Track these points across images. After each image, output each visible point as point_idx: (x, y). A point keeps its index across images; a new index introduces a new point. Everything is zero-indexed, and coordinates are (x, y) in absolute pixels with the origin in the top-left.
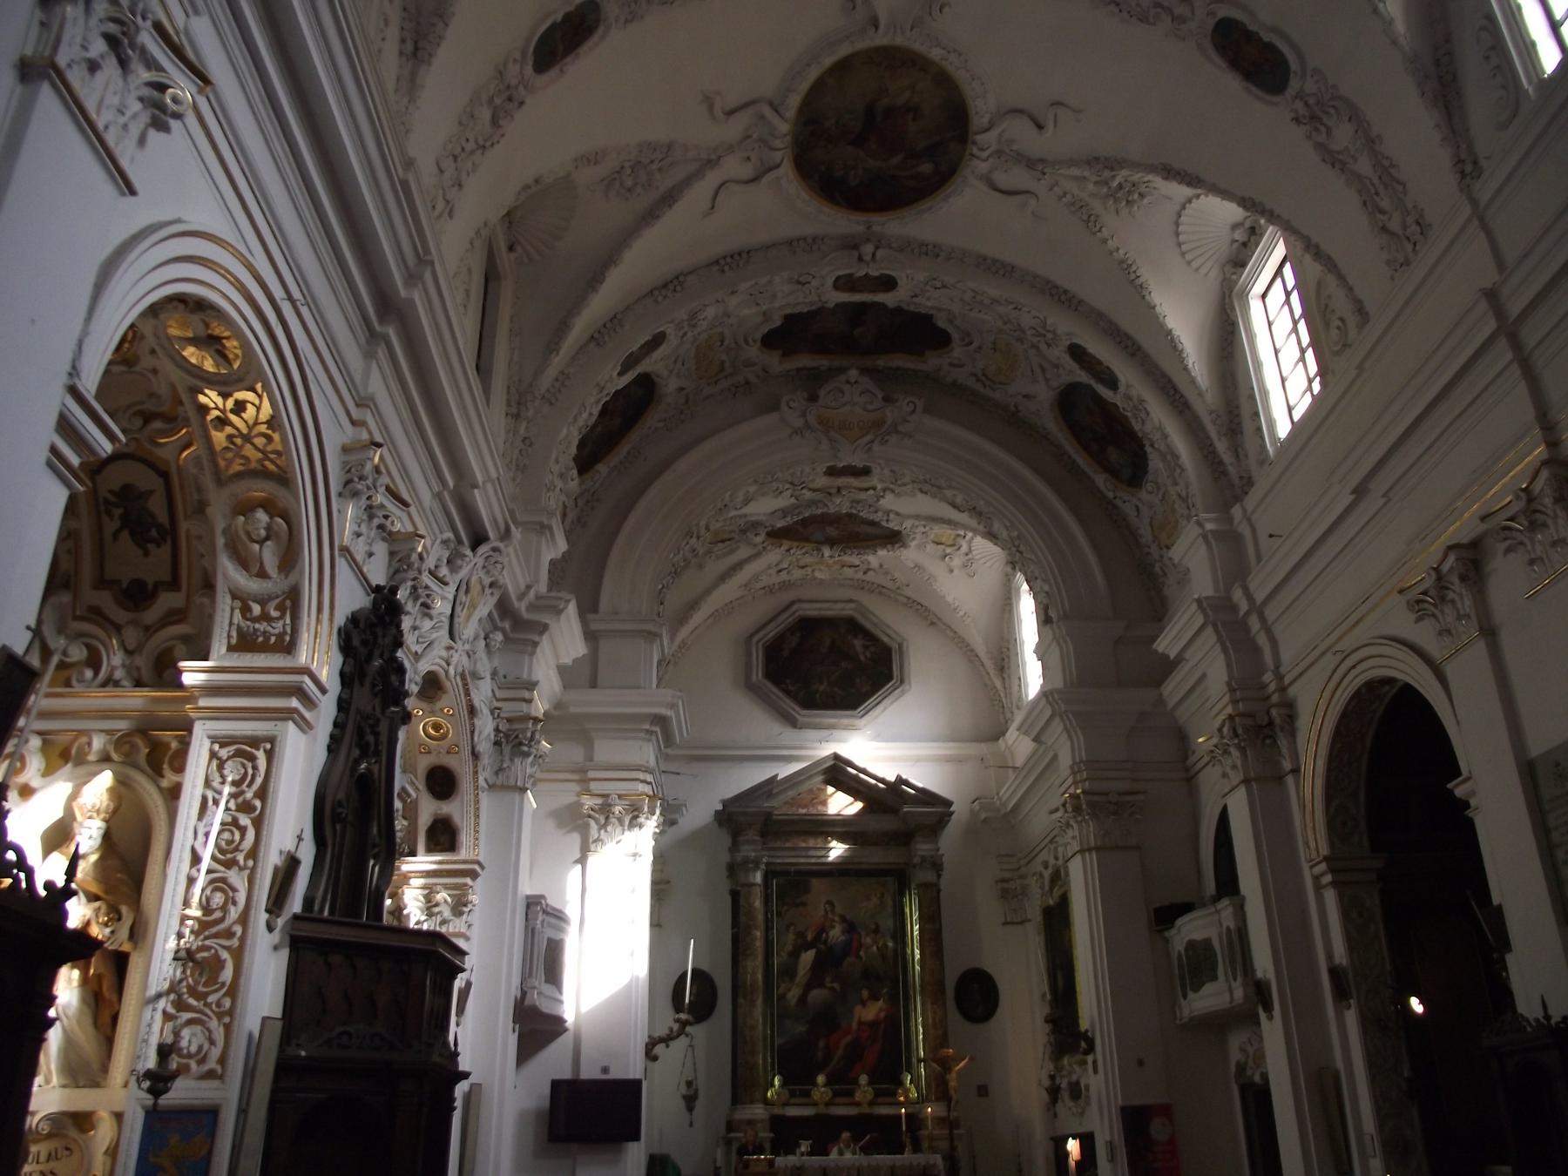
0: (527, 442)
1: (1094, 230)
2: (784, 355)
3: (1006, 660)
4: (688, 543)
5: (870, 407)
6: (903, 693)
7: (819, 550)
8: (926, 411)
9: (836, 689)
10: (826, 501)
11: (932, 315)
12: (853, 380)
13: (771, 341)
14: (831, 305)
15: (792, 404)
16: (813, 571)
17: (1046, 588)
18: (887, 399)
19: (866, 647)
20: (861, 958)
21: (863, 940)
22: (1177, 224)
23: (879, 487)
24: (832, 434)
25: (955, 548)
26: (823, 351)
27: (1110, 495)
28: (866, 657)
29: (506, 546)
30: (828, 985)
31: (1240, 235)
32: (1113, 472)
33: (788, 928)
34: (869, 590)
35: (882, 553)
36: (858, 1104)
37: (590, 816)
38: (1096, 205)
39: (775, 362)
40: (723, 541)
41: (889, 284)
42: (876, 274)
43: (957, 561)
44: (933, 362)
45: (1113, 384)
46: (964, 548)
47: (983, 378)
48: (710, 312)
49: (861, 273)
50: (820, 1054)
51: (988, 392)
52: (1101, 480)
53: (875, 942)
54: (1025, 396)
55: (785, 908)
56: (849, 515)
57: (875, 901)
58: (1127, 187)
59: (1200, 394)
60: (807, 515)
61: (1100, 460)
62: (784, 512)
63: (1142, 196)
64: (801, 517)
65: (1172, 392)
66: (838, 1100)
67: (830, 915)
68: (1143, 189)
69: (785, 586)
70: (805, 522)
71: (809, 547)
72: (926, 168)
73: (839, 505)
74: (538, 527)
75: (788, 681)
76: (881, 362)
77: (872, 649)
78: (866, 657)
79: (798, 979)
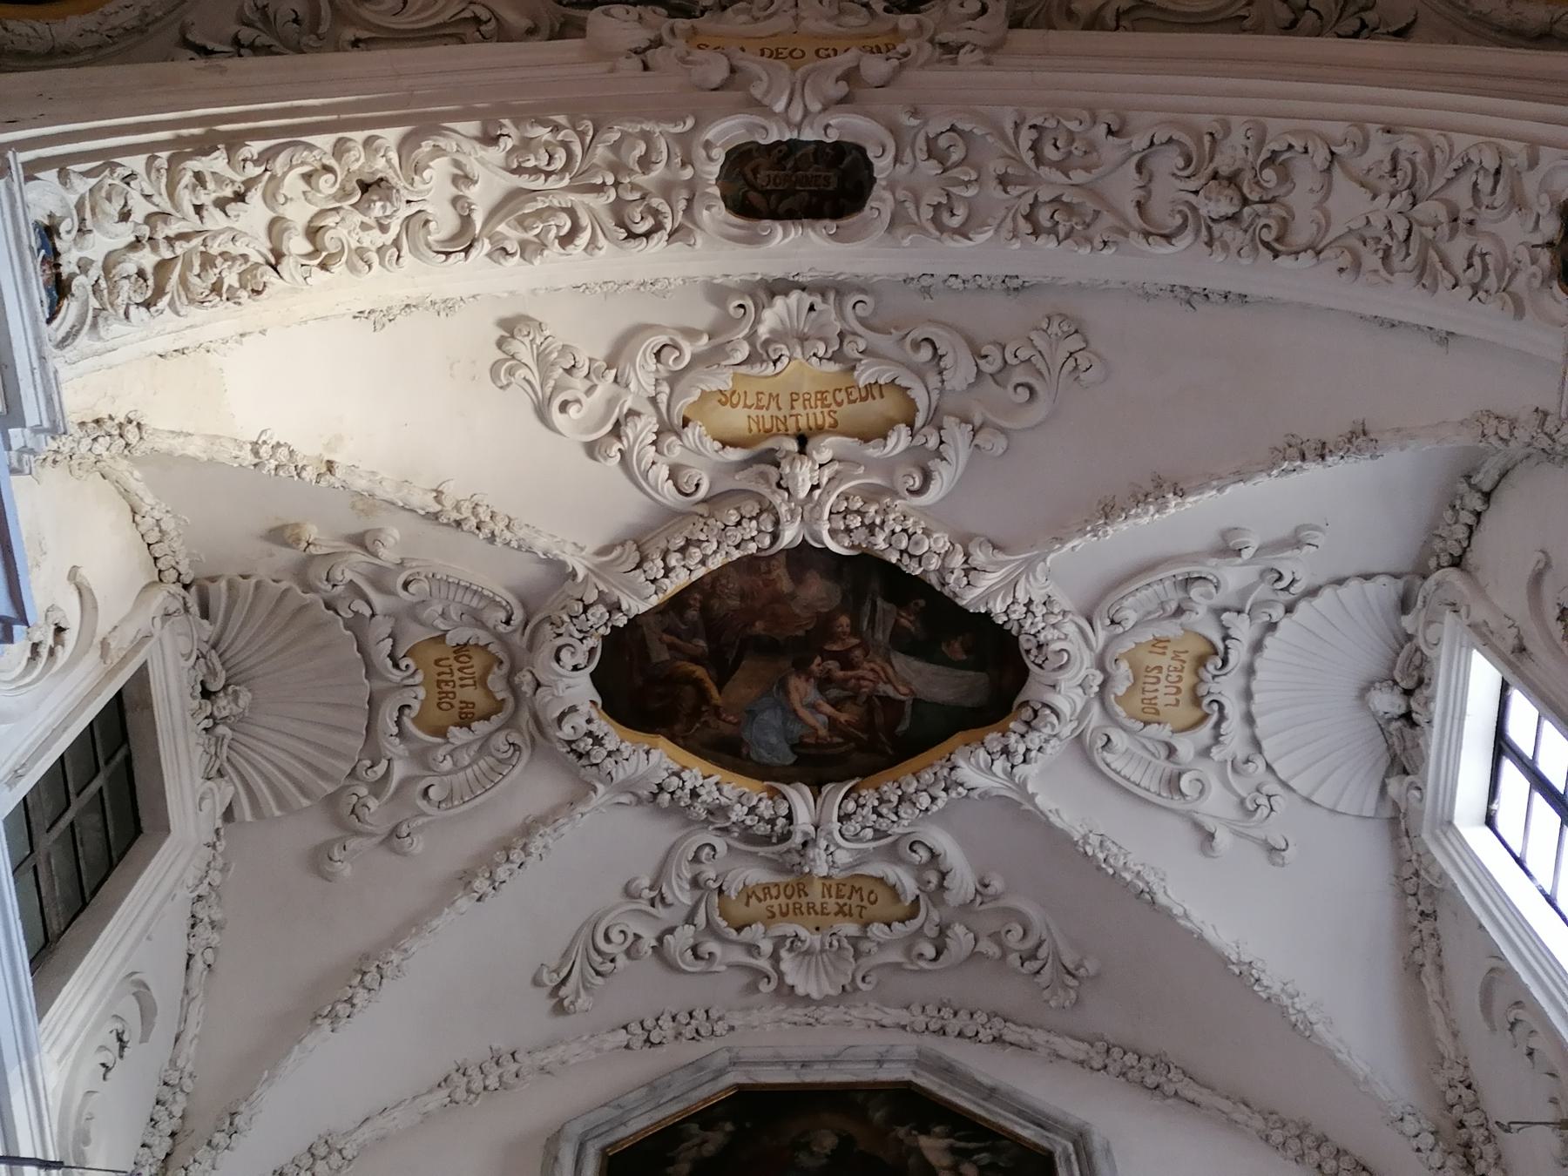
7: (774, 794)
10: (764, 490)
19: (961, 1155)
34: (960, 1034)
40: (465, 722)
69: (691, 1024)
77: (984, 1158)
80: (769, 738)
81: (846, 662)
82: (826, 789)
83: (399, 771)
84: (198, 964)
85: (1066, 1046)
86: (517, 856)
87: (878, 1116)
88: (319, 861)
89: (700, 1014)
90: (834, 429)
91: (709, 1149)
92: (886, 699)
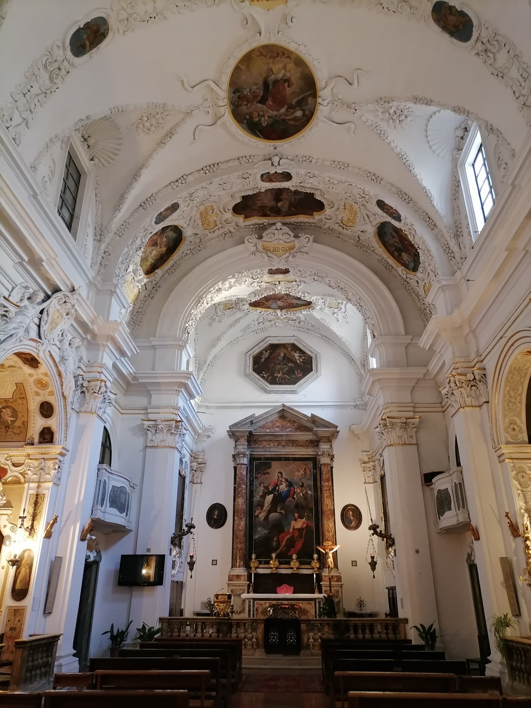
0: (107, 254)
1: (383, 138)
2: (246, 217)
3: (366, 361)
4: (201, 306)
5: (288, 241)
6: (317, 377)
8: (315, 241)
9: (285, 376)
11: (313, 194)
12: (279, 228)
13: (238, 209)
14: (263, 190)
15: (250, 240)
16: (275, 323)
17: (373, 322)
18: (296, 236)
20: (294, 498)
21: (296, 490)
22: (426, 131)
23: (298, 280)
24: (269, 254)
25: (339, 309)
26: (265, 215)
27: (405, 277)
28: (300, 361)
29: (72, 295)
30: (279, 511)
31: (460, 133)
32: (406, 266)
33: (260, 485)
35: (304, 312)
36: (292, 568)
37: (148, 430)
38: (383, 125)
39: (240, 219)
41: (287, 177)
42: (281, 172)
43: (340, 316)
44: (317, 217)
45: (398, 218)
46: (343, 310)
47: (342, 224)
48: (201, 193)
49: (272, 172)
50: (275, 544)
51: (345, 231)
52: (400, 269)
53: (302, 491)
54: (362, 232)
55: (259, 475)
56: (287, 295)
57: (302, 472)
58: (398, 112)
59: (441, 218)
60: (266, 295)
61: (399, 259)
62: (255, 293)
63: (406, 117)
64: (264, 296)
65: (428, 219)
66: (282, 566)
67: (280, 478)
68: (406, 112)
70: (267, 299)
71: (271, 311)
72: (299, 113)
73: (281, 289)
74: (109, 292)
75: (264, 372)
76: (293, 219)
78: (300, 361)
79: (264, 509)
80: (274, 305)
81: (286, 300)
82: (283, 310)
83: (220, 314)
84: (196, 340)
85: (317, 335)
86: (238, 323)
87: (289, 349)
88: (210, 325)
89: (264, 329)
90: (284, 281)
91: (267, 356)
92: (292, 303)
